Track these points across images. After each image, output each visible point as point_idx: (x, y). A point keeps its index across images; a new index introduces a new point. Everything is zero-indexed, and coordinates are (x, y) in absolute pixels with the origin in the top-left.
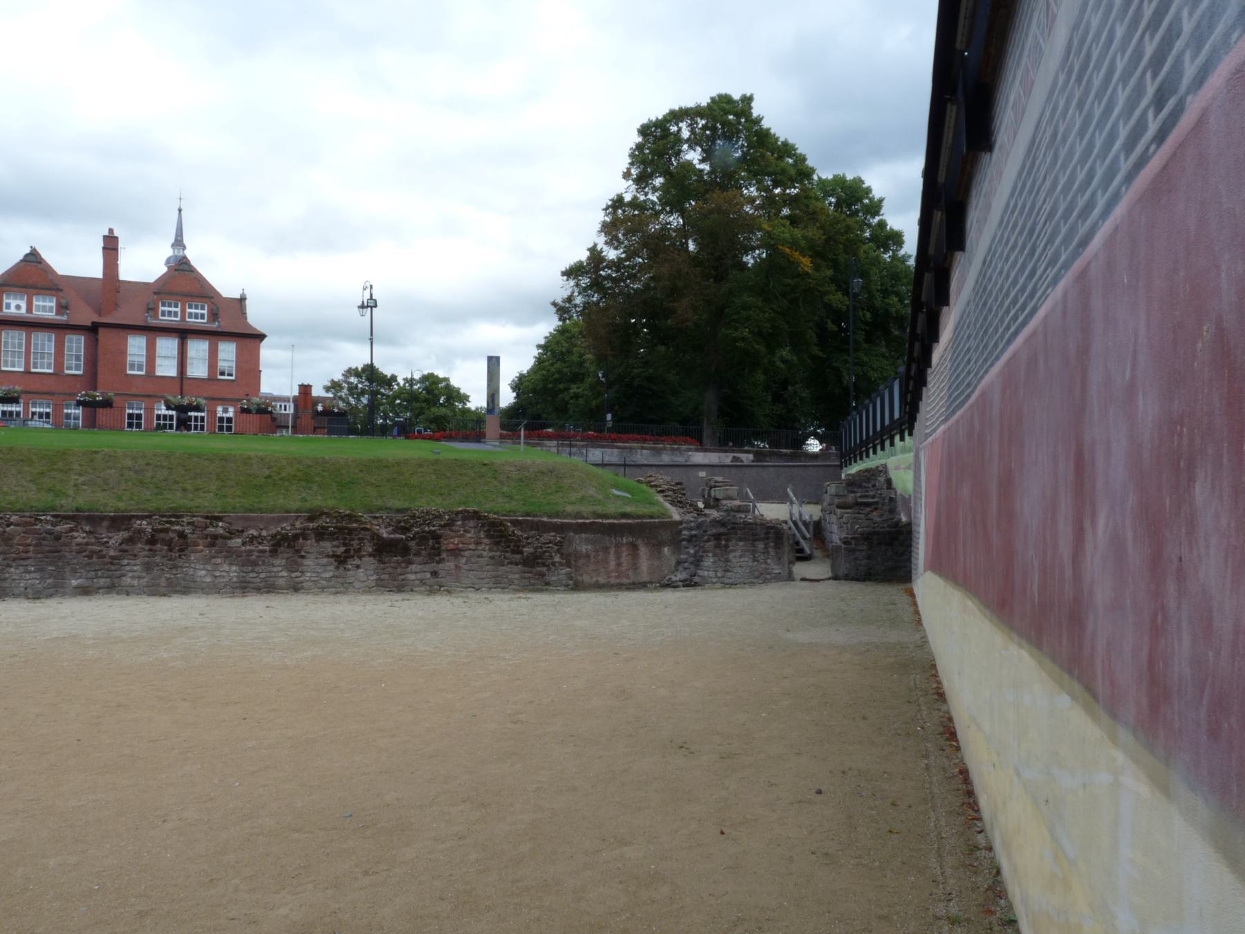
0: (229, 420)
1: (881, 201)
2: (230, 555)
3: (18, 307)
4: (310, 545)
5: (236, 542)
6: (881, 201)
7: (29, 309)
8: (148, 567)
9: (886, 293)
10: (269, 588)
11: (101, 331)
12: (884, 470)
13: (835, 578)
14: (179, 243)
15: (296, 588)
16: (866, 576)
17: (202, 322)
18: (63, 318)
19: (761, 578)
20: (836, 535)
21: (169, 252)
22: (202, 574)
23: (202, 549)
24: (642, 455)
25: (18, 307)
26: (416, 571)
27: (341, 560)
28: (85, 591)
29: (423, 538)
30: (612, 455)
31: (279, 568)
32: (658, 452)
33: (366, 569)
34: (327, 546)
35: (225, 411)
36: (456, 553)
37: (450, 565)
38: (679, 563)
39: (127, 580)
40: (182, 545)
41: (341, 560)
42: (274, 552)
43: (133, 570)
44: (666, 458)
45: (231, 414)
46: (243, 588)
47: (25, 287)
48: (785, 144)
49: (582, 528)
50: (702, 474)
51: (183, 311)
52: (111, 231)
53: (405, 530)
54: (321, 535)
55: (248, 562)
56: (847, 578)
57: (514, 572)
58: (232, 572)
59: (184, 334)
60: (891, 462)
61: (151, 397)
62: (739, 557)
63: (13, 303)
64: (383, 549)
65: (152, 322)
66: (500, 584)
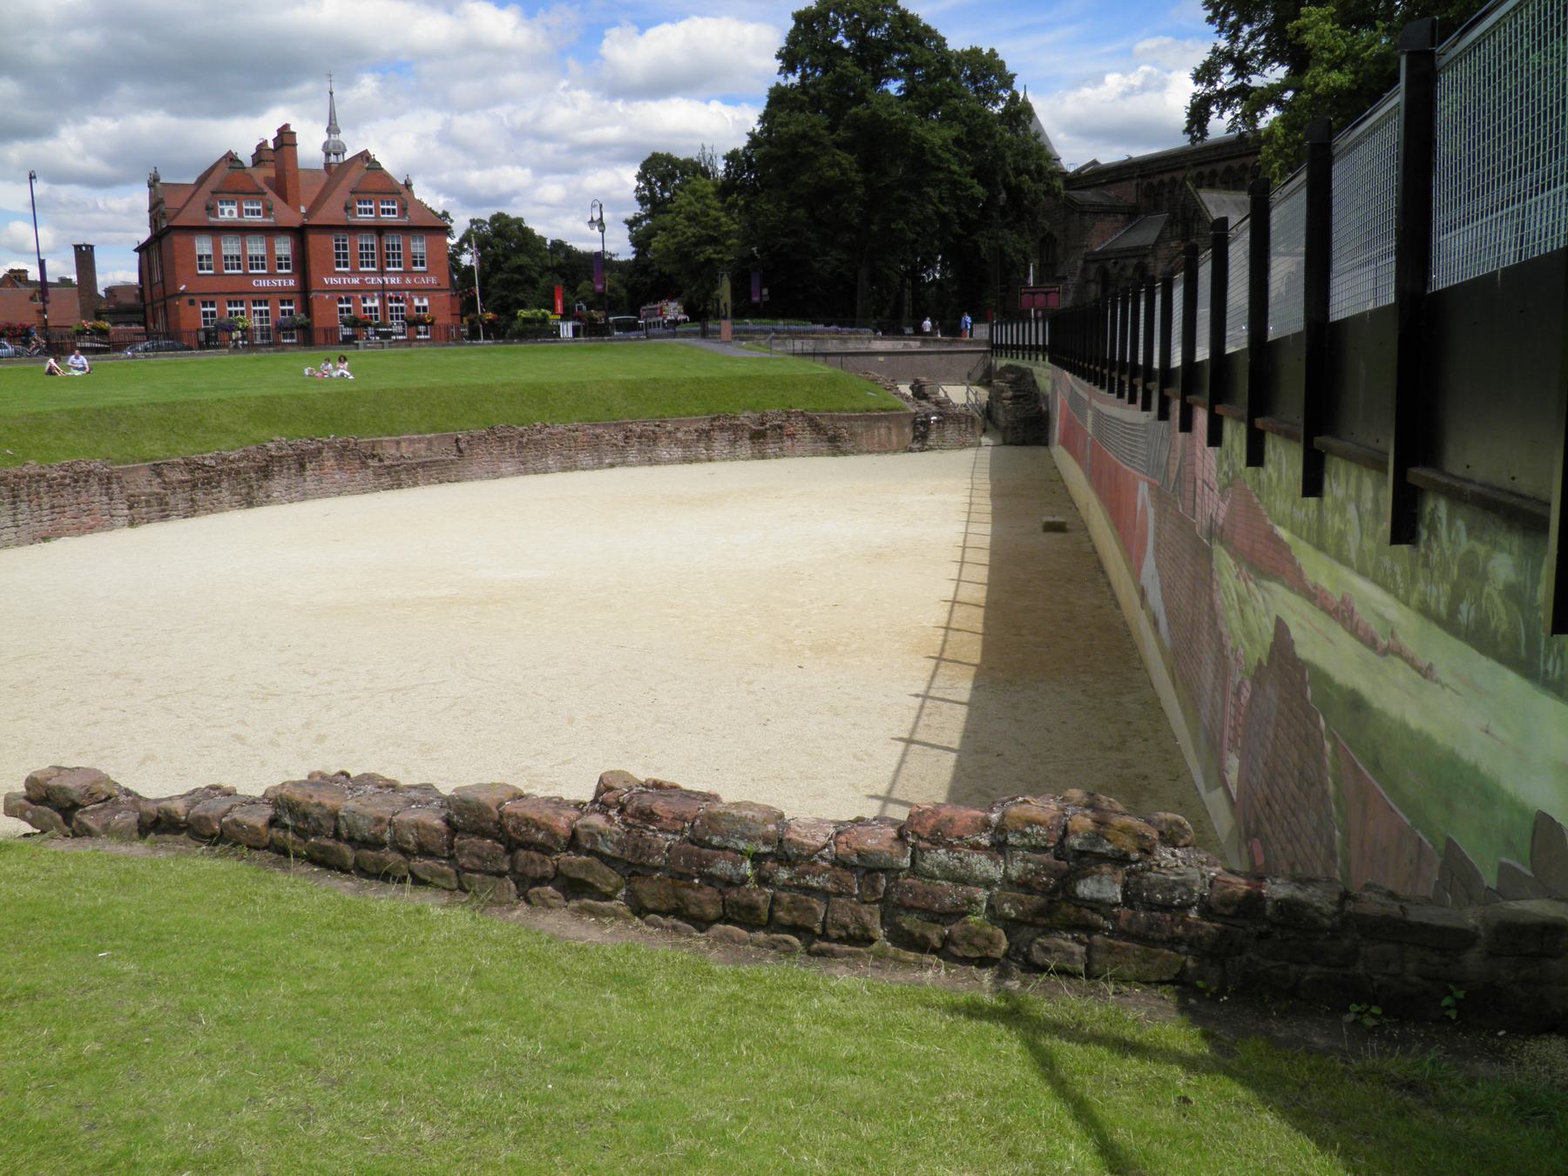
0: (425, 309)
1: (1013, 76)
2: (678, 443)
3: (231, 212)
4: (716, 434)
5: (679, 435)
6: (1013, 76)
7: (240, 215)
9: (1019, 172)
12: (1031, 373)
13: (1005, 443)
15: (710, 460)
16: (1024, 443)
17: (392, 219)
18: (270, 221)
19: (963, 446)
20: (1002, 417)
21: (325, 137)
22: (665, 454)
23: (665, 441)
24: (833, 345)
25: (231, 212)
26: (771, 448)
28: (612, 466)
29: (774, 428)
30: (809, 345)
32: (844, 340)
33: (745, 446)
35: (421, 300)
36: (792, 436)
38: (915, 438)
40: (654, 439)
42: (698, 441)
43: (632, 454)
44: (852, 346)
45: (426, 303)
47: (236, 192)
48: (927, 29)
49: (856, 419)
50: (881, 359)
51: (377, 207)
52: (286, 126)
53: (763, 424)
54: (722, 429)
55: (685, 445)
56: (1011, 444)
57: (824, 446)
58: (678, 452)
59: (380, 230)
60: (1036, 370)
62: (950, 432)
63: (227, 208)
64: (758, 436)
65: (353, 220)
66: (816, 453)
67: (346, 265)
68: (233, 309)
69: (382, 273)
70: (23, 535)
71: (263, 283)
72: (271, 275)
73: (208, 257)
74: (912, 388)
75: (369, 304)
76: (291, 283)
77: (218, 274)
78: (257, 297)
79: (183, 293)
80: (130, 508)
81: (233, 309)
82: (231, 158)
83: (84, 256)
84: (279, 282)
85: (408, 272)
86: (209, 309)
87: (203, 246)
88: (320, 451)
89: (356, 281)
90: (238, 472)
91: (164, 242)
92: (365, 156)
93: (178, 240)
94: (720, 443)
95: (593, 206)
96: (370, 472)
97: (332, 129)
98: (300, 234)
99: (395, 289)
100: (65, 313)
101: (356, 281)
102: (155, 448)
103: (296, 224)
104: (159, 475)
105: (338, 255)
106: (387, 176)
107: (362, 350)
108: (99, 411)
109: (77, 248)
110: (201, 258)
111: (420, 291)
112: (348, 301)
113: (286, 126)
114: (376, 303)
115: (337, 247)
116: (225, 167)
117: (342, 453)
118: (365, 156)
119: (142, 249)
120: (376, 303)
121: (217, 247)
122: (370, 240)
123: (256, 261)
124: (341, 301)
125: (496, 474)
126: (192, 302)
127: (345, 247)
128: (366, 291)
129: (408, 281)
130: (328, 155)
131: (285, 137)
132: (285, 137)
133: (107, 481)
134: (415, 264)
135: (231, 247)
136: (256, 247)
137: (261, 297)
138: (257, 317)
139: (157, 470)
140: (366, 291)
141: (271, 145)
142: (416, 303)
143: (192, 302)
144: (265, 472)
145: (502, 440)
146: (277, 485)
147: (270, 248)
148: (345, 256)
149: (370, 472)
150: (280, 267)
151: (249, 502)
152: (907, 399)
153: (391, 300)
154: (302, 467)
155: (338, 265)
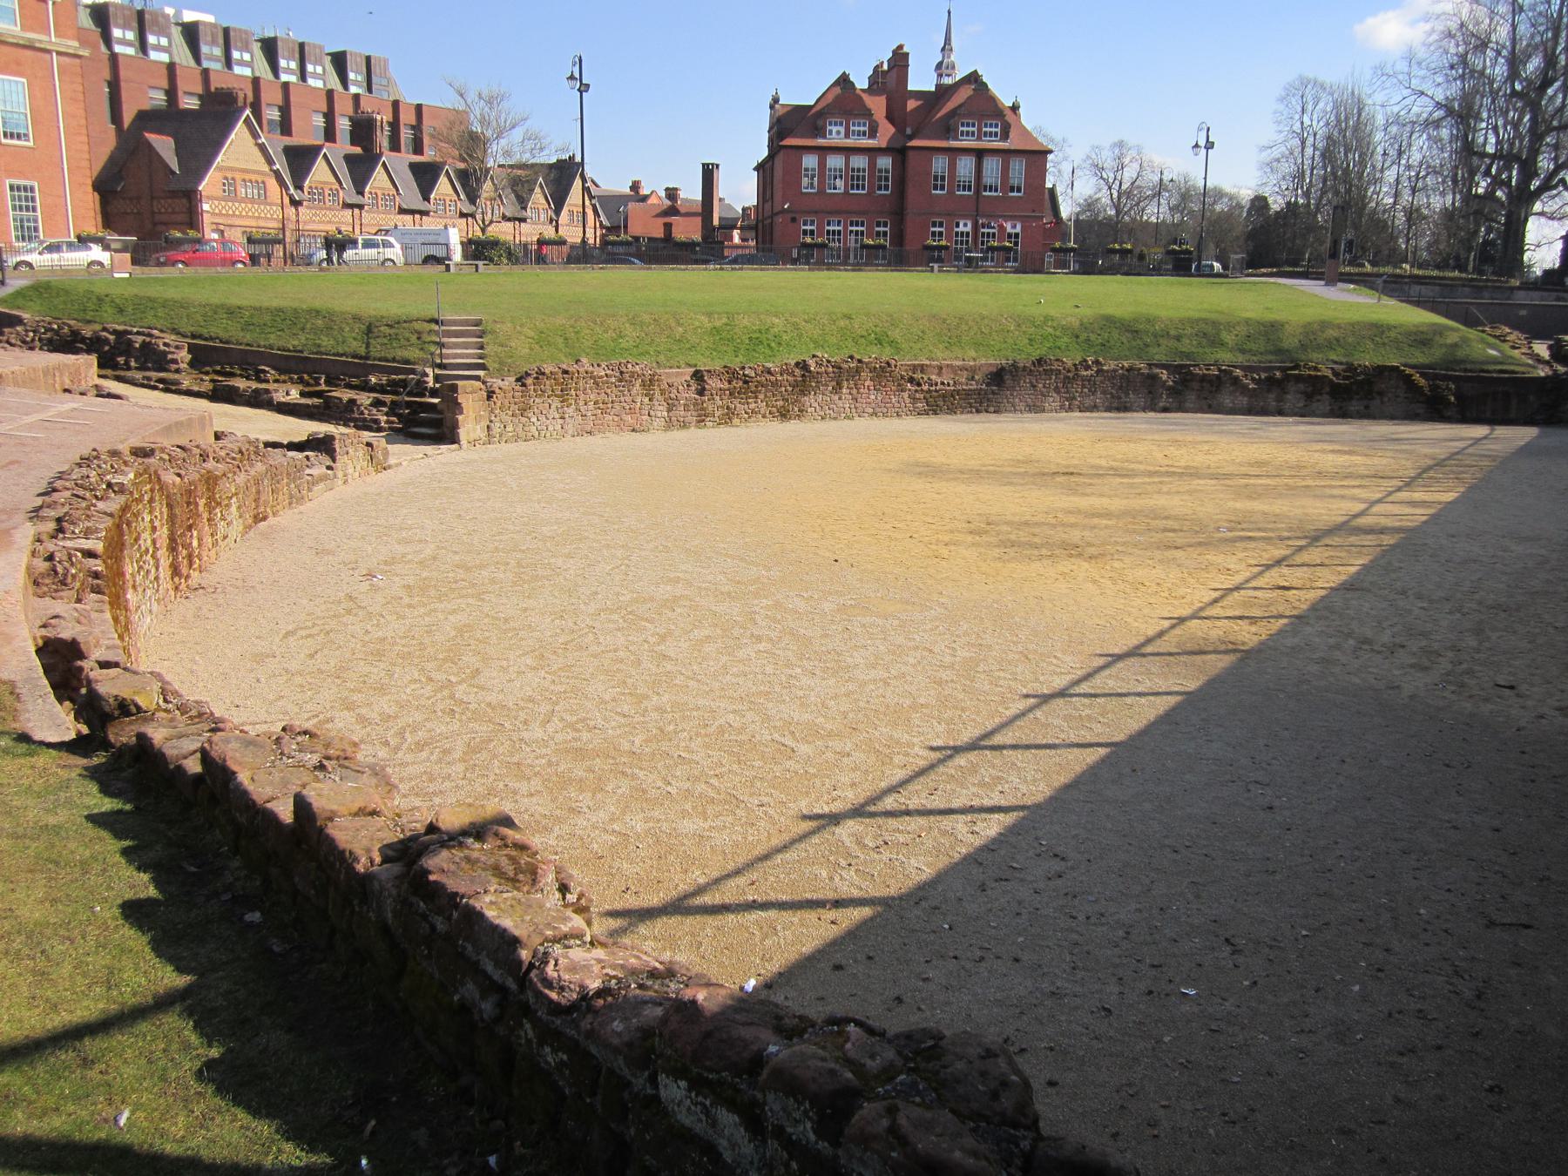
0: (1017, 235)
4: (1292, 387)
7: (847, 136)
8: (1199, 397)
10: (1263, 412)
11: (911, 154)
14: (947, 47)
15: (1281, 413)
22: (1227, 401)
26: (1355, 406)
27: (1309, 396)
28: (1165, 410)
31: (1271, 400)
33: (1325, 402)
34: (1301, 386)
35: (1014, 227)
37: (1377, 402)
39: (1188, 405)
41: (1309, 396)
43: (1191, 397)
45: (1018, 229)
46: (1250, 411)
51: (980, 130)
58: (1244, 401)
59: (980, 154)
61: (953, 216)
67: (942, 188)
70: (570, 429)
74: (1550, 348)
75: (961, 228)
77: (821, 192)
79: (783, 211)
80: (669, 411)
82: (844, 81)
83: (709, 173)
88: (858, 371)
90: (775, 384)
92: (974, 78)
94: (1293, 398)
95: (1200, 129)
96: (906, 395)
97: (947, 47)
100: (687, 230)
106: (993, 100)
113: (901, 47)
116: (838, 90)
117: (882, 373)
118: (974, 78)
119: (760, 168)
120: (969, 228)
125: (1035, 408)
130: (940, 76)
131: (900, 59)
132: (900, 59)
133: (649, 384)
134: (1012, 189)
141: (885, 67)
142: (1009, 230)
143: (794, 220)
145: (1048, 373)
146: (810, 400)
148: (943, 178)
149: (906, 395)
151: (784, 415)
152: (1538, 359)
154: (838, 388)
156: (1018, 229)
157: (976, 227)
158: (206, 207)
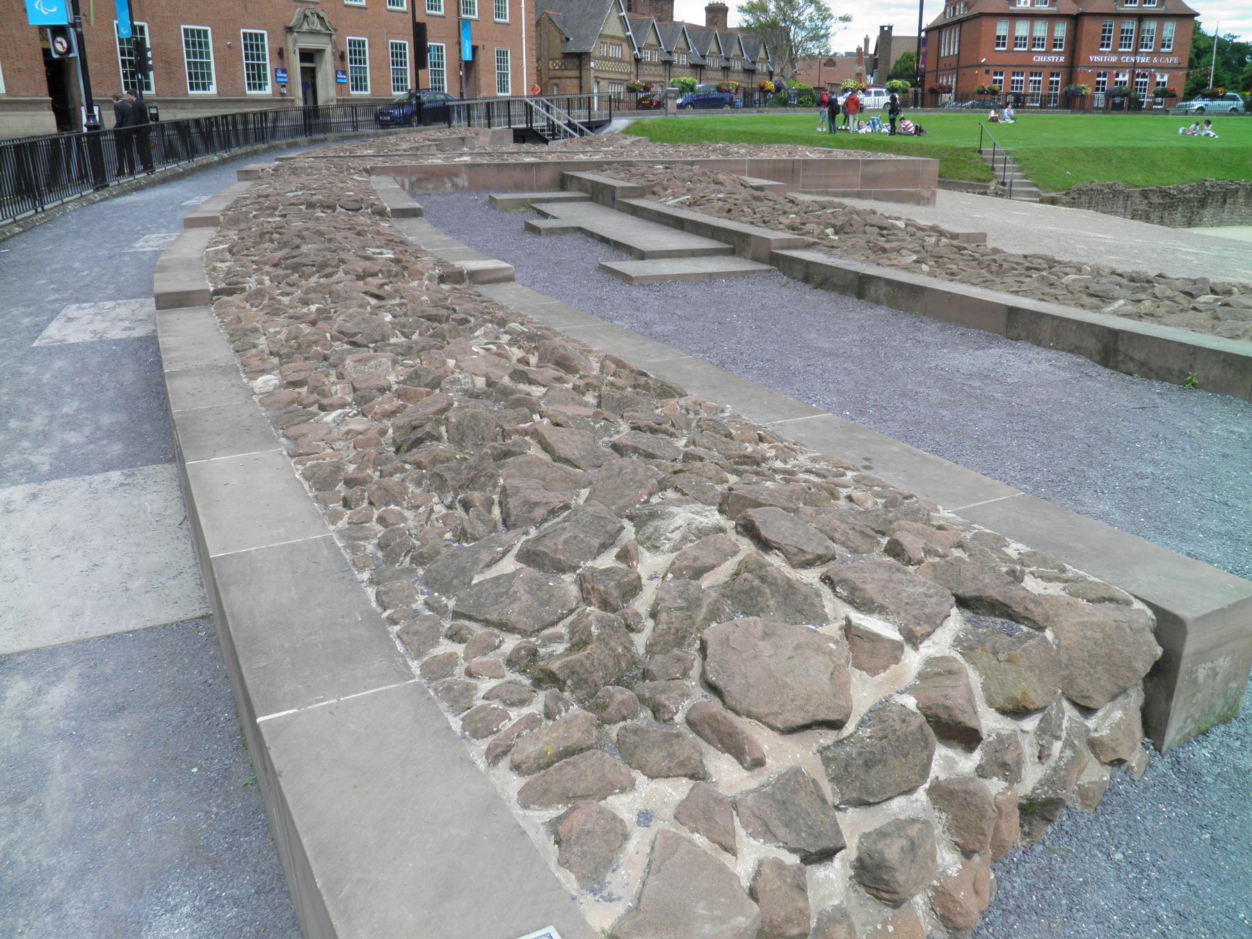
0: (1164, 83)
35: (1162, 77)
45: (1166, 79)
59: (1140, 17)
68: (1015, 78)
69: (1136, 53)
71: (1041, 59)
72: (1048, 53)
73: (1004, 38)
75: (1121, 78)
76: (1062, 59)
78: (1034, 70)
79: (983, 65)
81: (1015, 78)
84: (1052, 59)
85: (1156, 53)
86: (998, 78)
87: (1002, 29)
88: (1237, 190)
89: (1114, 59)
90: (1189, 201)
91: (964, 25)
93: (986, 23)
98: (1075, 20)
99: (1143, 66)
101: (1114, 59)
102: (1139, 179)
103: (1074, 12)
104: (1146, 198)
105: (1103, 38)
107: (1170, 117)
108: (1097, 150)
109: (882, 28)
110: (998, 38)
111: (1162, 68)
112: (1105, 75)
114: (1126, 78)
115: (1104, 31)
120: (1126, 78)
121: (1012, 29)
122: (1130, 25)
123: (1035, 41)
124: (1099, 75)
126: (987, 72)
127: (1110, 31)
128: (1120, 67)
129: (1155, 60)
134: (1163, 46)
135: (1022, 29)
136: (1041, 29)
137: (1037, 69)
138: (1031, 85)
139: (1145, 194)
140: (1120, 67)
142: (1158, 79)
144: (1203, 203)
146: (1208, 212)
147: (1051, 31)
148: (1109, 38)
150: (1055, 46)
151: (1190, 224)
153: (1138, 76)
155: (1102, 46)
156: (1166, 79)
157: (1132, 79)
158: (592, 65)
